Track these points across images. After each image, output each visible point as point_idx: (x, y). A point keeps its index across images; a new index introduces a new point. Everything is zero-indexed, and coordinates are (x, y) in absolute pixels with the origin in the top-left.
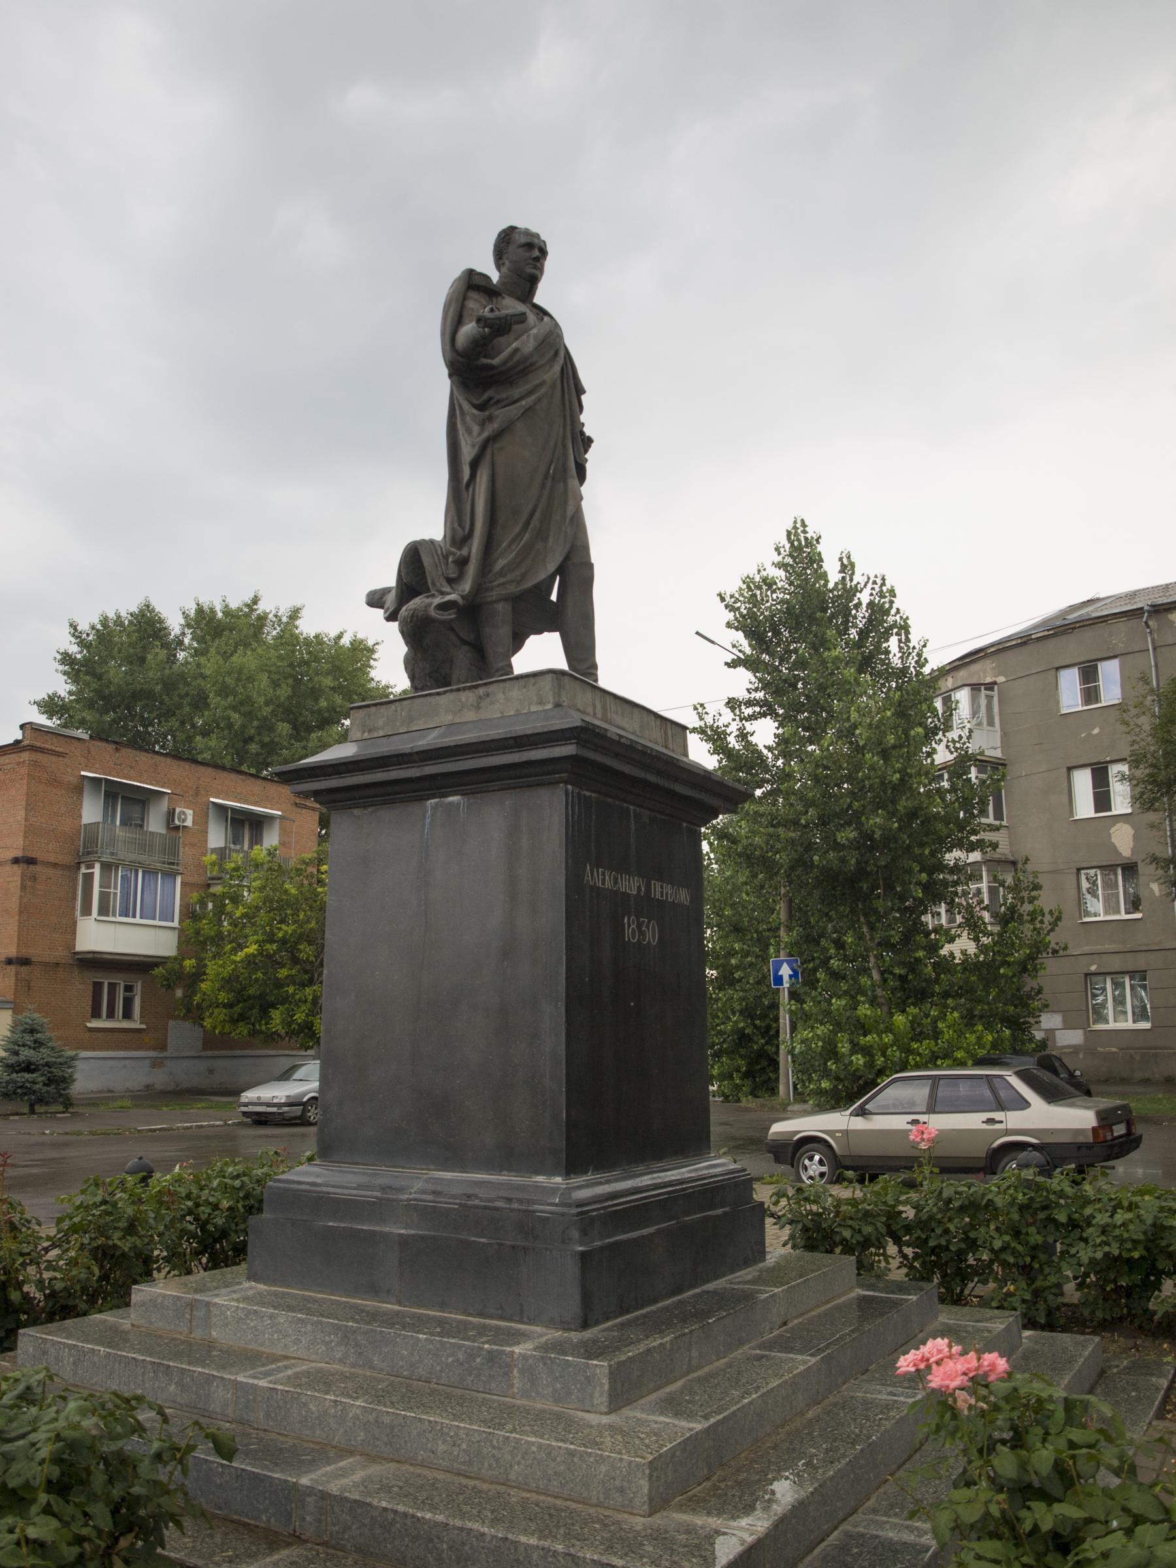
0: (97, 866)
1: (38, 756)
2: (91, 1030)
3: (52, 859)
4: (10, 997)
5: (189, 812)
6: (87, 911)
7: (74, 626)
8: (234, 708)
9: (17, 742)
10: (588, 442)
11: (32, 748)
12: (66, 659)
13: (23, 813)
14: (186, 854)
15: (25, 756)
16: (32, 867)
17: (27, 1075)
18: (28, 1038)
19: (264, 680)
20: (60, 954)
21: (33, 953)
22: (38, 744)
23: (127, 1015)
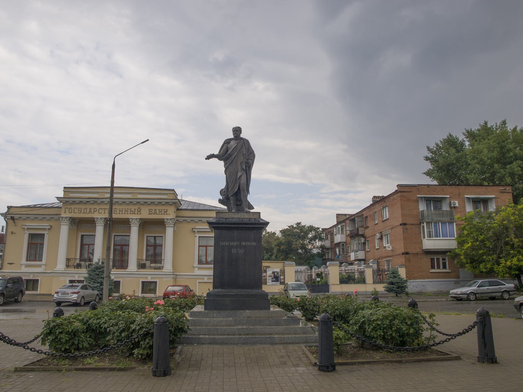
0: (425, 223)
1: (403, 194)
2: (431, 273)
3: (411, 223)
5: (457, 202)
6: (424, 237)
7: (428, 148)
8: (478, 163)
9: (396, 191)
11: (400, 192)
12: (427, 159)
14: (457, 216)
15: (399, 194)
16: (406, 226)
18: (392, 276)
19: (486, 151)
20: (418, 250)
21: (408, 251)
23: (444, 267)
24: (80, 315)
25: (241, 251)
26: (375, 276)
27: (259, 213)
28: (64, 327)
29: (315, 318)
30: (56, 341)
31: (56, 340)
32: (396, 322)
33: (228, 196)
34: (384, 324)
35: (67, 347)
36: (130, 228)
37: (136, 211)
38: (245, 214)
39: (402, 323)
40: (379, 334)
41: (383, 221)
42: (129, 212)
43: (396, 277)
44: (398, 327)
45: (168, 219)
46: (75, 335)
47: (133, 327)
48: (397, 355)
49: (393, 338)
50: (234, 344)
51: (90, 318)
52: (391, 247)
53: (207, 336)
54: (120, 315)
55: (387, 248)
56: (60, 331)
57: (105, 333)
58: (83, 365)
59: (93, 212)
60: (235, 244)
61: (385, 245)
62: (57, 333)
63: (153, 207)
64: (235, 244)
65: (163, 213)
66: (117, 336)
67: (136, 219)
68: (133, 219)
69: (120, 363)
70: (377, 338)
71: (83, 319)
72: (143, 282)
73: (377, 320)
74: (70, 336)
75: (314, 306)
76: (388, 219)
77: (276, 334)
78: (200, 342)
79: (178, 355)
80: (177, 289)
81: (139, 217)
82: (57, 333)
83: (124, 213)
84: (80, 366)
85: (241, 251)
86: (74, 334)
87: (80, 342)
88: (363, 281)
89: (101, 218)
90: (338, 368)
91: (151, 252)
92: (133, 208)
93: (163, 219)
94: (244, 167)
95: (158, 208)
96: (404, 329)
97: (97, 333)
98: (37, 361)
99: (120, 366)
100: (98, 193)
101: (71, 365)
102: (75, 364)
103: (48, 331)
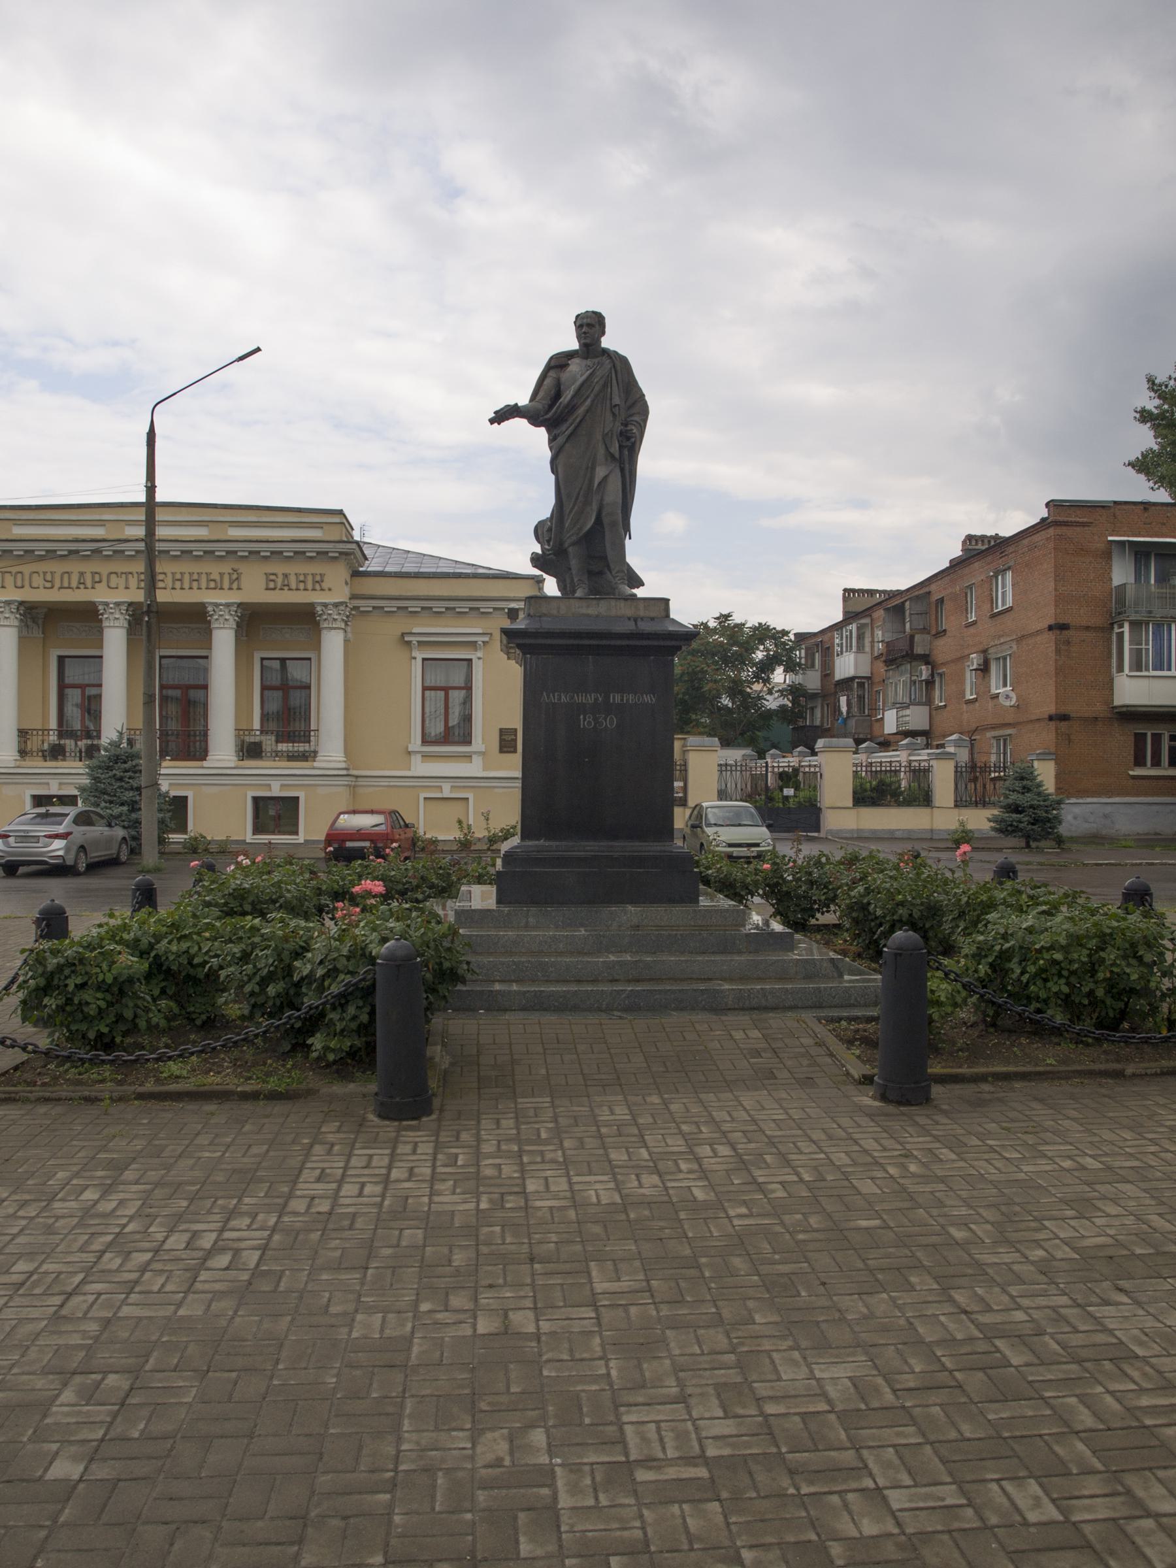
0: (1126, 628)
2: (1134, 777)
3: (1084, 623)
4: (1053, 750)
6: (1120, 669)
9: (1043, 520)
10: (540, 531)
11: (1056, 524)
13: (1052, 584)
15: (1051, 531)
17: (1014, 816)
18: (1018, 785)
20: (1099, 709)
22: (1061, 519)
24: (125, 927)
25: (610, 723)
26: (962, 787)
27: (666, 601)
28: (88, 968)
29: (813, 921)
30: (71, 1011)
31: (68, 1008)
32: (1110, 955)
33: (561, 544)
34: (1071, 962)
35: (105, 1030)
36: (209, 632)
37: (226, 578)
38: (622, 604)
39: (1125, 957)
40: (1055, 989)
41: (994, 616)
42: (204, 585)
43: (1029, 790)
44: (1116, 970)
45: (325, 605)
46: (122, 992)
47: (303, 968)
48: (1105, 1052)
49: (1094, 1002)
50: (600, 1010)
51: (158, 938)
52: (1013, 695)
53: (515, 987)
54: (254, 930)
55: (1001, 699)
56: (79, 981)
57: (210, 982)
58: (158, 1081)
59: (89, 585)
60: (590, 699)
61: (994, 691)
62: (71, 988)
63: (279, 568)
64: (590, 699)
65: (310, 586)
66: (252, 994)
67: (228, 605)
68: (217, 605)
69: (268, 1074)
70: (1046, 1001)
71: (137, 940)
72: (256, 800)
73: (1051, 948)
74: (109, 997)
75: (811, 883)
76: (1010, 609)
77: (724, 979)
78: (496, 1005)
79: (439, 1047)
80: (365, 821)
81: (235, 597)
82: (71, 988)
83: (186, 585)
84: (150, 1086)
85: (610, 723)
86: (120, 989)
87: (139, 1011)
88: (922, 797)
89: (118, 604)
90: (937, 1090)
91: (274, 706)
92: (215, 569)
93: (312, 605)
94: (615, 449)
95: (293, 569)
96: (1134, 977)
97: (183, 984)
98: (16, 1068)
99: (272, 1084)
100: (101, 523)
101: (120, 1083)
102: (130, 1079)
103: (42, 982)
